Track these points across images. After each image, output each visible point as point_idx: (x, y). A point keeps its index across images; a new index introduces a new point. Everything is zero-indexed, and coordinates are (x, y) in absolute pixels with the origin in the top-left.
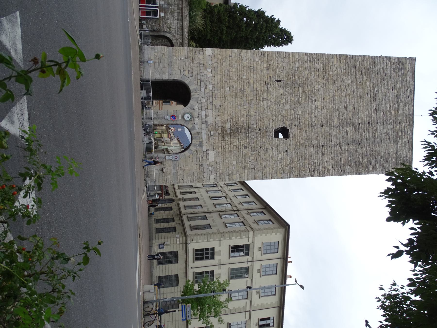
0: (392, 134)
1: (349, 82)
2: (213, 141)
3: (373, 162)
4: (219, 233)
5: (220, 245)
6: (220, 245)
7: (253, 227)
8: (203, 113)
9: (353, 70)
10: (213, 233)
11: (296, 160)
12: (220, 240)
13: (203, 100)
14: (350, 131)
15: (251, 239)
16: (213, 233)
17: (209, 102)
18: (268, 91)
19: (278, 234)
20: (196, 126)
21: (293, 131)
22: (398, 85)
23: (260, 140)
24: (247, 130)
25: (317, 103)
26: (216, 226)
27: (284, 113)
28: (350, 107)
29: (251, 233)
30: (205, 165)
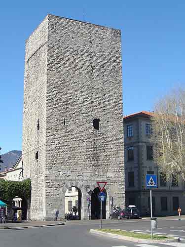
0: (98, 41)
1: (64, 69)
2: (102, 173)
3: (115, 59)
4: (139, 167)
5: (146, 167)
6: (146, 167)
7: (135, 141)
8: (85, 179)
9: (56, 65)
10: (138, 171)
11: (113, 116)
12: (144, 167)
13: (77, 178)
14: (96, 73)
15: (144, 144)
16: (138, 171)
17: (78, 175)
18: (72, 131)
19: (142, 124)
20: (93, 184)
21: (96, 115)
22: (66, 30)
23: (101, 140)
24: (96, 149)
25: (79, 94)
26: (131, 168)
27: (85, 120)
28: (81, 71)
29: (140, 144)
30: (115, 179)
